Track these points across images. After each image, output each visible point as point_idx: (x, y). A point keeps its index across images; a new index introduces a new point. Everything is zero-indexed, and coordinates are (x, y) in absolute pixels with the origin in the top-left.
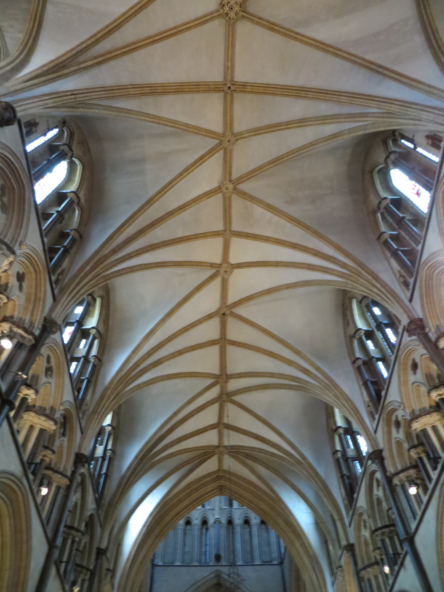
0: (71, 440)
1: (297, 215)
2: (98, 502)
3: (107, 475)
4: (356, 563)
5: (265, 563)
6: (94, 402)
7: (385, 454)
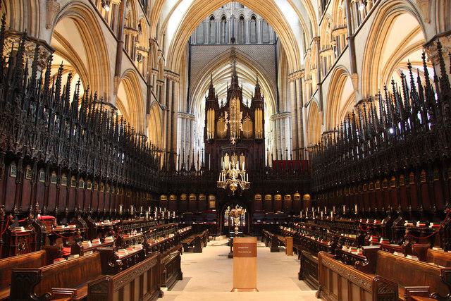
4: (319, 49)
5: (264, 44)
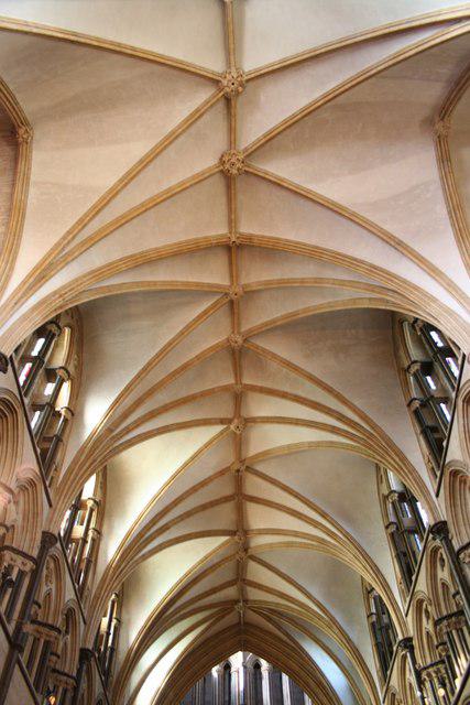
0: (74, 636)
1: (317, 374)
2: (105, 685)
3: (112, 649)
6: (95, 586)
7: (415, 643)
